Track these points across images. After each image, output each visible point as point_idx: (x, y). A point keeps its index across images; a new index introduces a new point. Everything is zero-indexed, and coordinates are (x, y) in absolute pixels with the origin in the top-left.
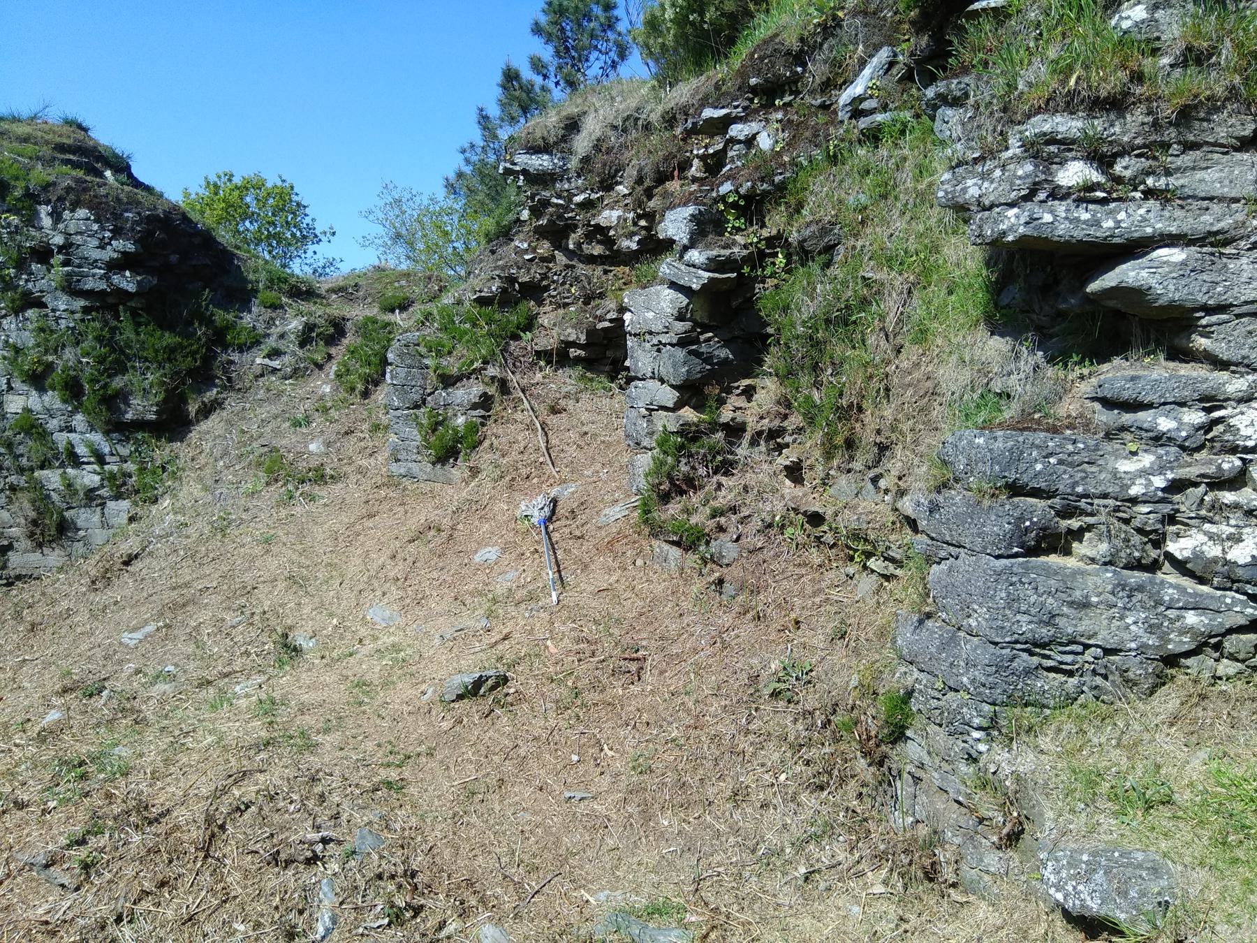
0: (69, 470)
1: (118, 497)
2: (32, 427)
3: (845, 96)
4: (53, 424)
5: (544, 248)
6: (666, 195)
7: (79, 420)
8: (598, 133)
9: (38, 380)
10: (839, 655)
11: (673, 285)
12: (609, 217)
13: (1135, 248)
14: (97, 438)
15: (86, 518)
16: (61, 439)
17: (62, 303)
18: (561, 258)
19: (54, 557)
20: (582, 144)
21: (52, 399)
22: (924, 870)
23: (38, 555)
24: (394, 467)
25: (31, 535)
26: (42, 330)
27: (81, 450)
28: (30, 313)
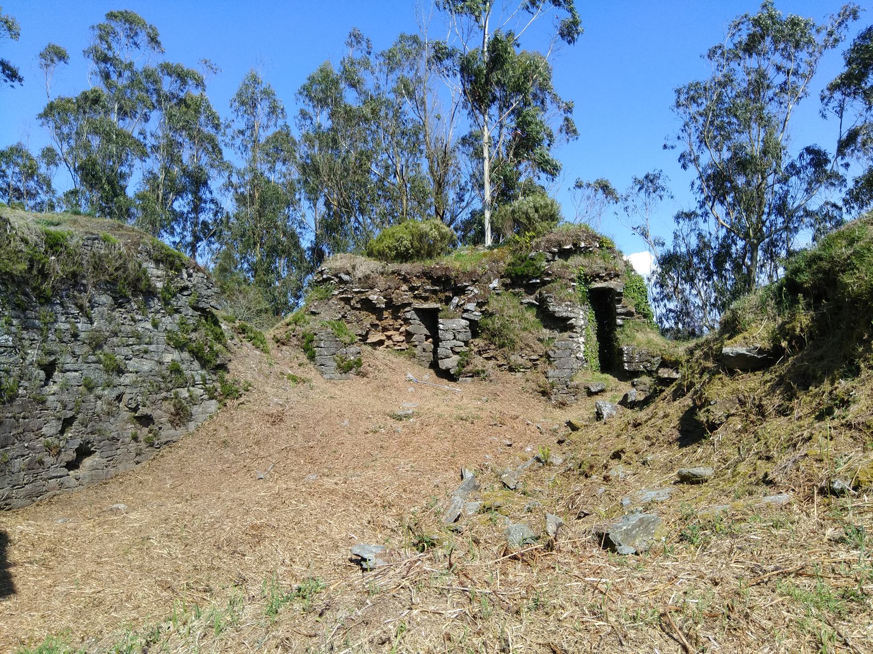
0: (191, 388)
1: (211, 398)
2: (176, 370)
3: (491, 286)
4: (183, 367)
5: (343, 303)
6: (397, 294)
7: (196, 364)
8: (368, 272)
9: (180, 347)
10: (528, 384)
11: (463, 318)
12: (373, 297)
13: (571, 318)
14: (204, 372)
15: (195, 409)
16: (188, 373)
17: (190, 312)
18: (348, 307)
19: (181, 431)
20: (359, 274)
21: (186, 355)
22: (562, 405)
23: (173, 431)
24: (325, 376)
25: (172, 422)
26: (182, 324)
27: (198, 378)
28: (177, 316)
